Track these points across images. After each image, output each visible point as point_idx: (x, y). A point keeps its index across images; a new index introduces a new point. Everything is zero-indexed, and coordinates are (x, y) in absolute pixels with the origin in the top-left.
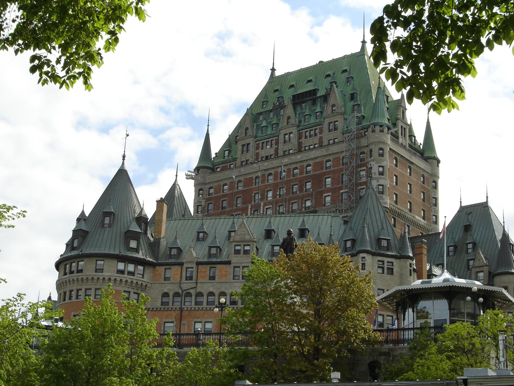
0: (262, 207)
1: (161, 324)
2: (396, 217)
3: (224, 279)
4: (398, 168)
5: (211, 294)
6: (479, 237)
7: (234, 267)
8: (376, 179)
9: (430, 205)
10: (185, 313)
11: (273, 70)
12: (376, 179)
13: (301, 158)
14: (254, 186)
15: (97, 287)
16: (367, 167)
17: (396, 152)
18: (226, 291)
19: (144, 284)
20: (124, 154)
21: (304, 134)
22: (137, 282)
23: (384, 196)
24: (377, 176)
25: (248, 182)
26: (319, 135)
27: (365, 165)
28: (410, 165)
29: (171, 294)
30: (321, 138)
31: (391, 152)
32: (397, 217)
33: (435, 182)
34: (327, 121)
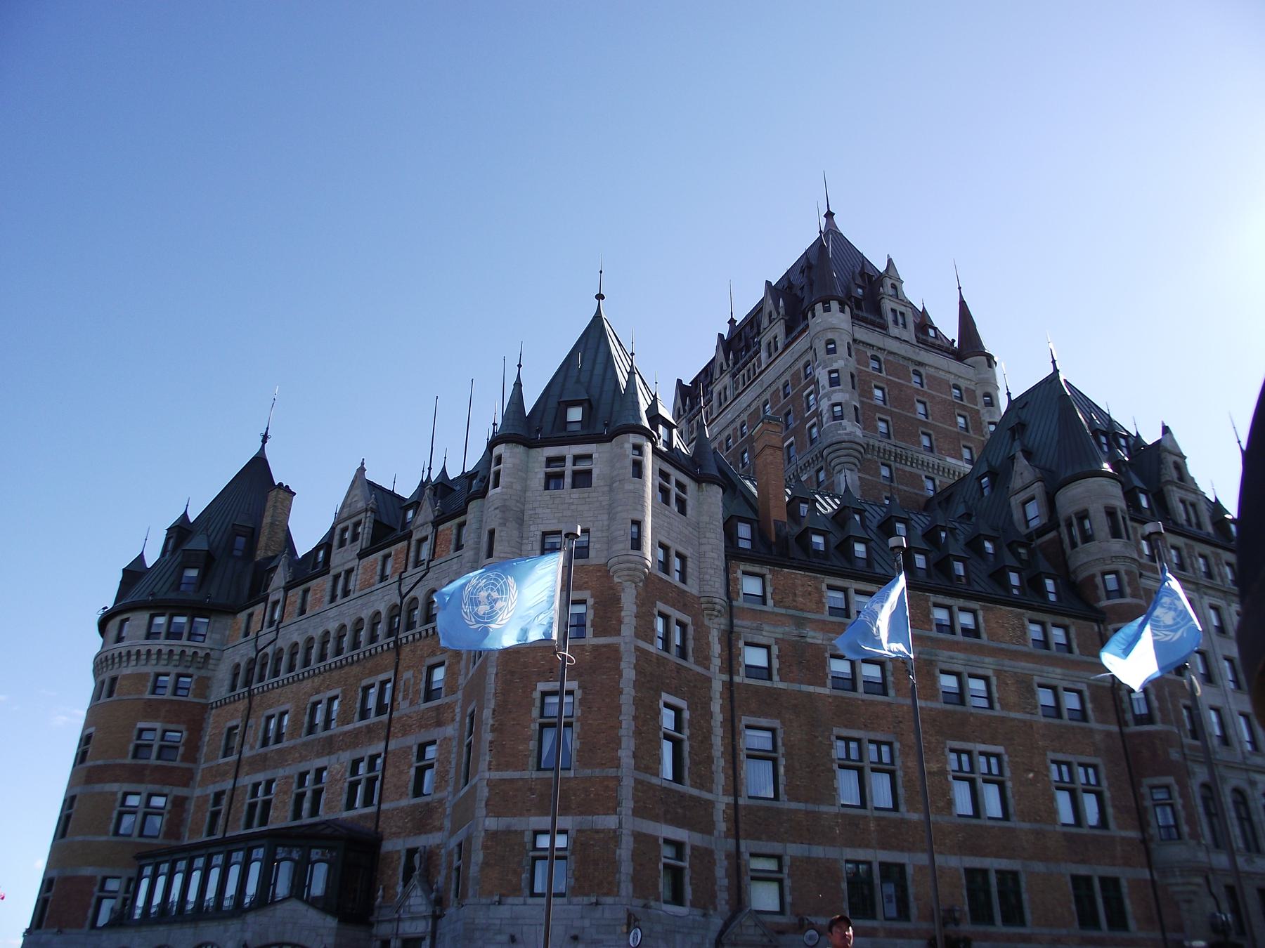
1: (223, 734)
2: (892, 463)
3: (317, 608)
4: (884, 374)
7: (337, 577)
9: (984, 436)
10: (257, 700)
13: (732, 416)
15: (112, 673)
17: (873, 346)
18: (314, 635)
19: (201, 653)
20: (266, 433)
22: (183, 652)
23: (844, 422)
28: (917, 368)
31: (861, 347)
32: (895, 461)
33: (987, 395)
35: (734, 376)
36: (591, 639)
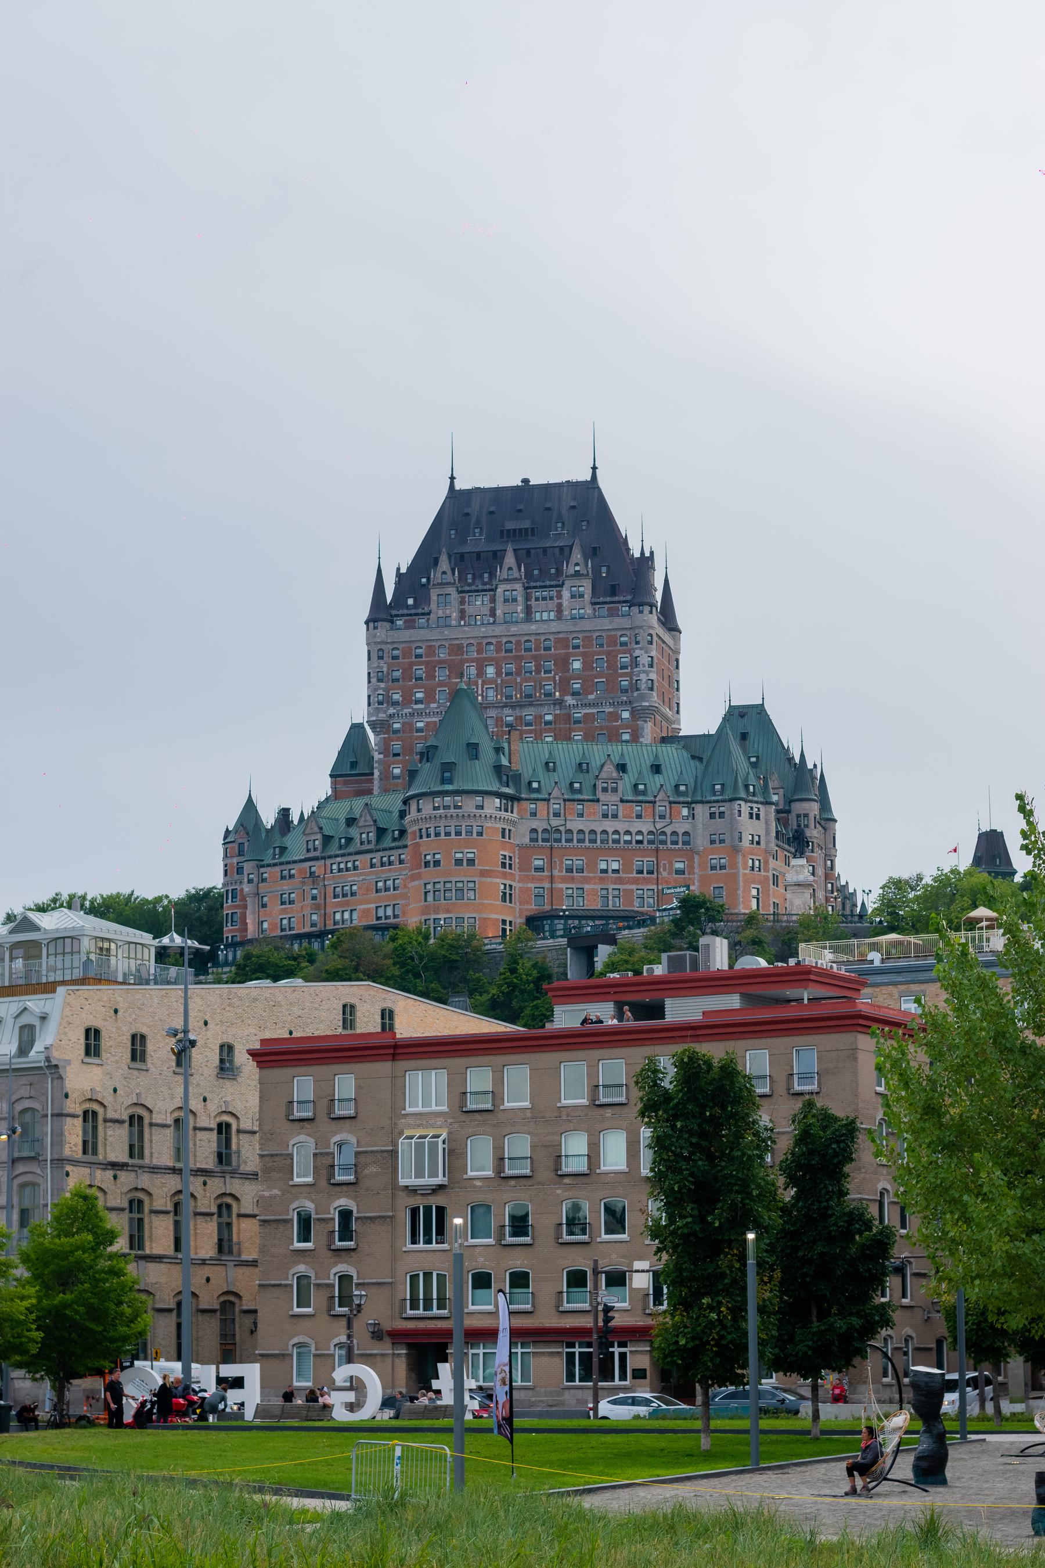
0: (480, 686)
5: (581, 831)
6: (760, 749)
8: (644, 672)
11: (452, 478)
12: (644, 672)
14: (465, 656)
16: (631, 655)
21: (533, 595)
24: (647, 668)
25: (457, 649)
26: (556, 601)
27: (630, 652)
29: (540, 831)
30: (560, 605)
33: (677, 661)
34: (568, 584)
35: (526, 588)
36: (763, 873)
